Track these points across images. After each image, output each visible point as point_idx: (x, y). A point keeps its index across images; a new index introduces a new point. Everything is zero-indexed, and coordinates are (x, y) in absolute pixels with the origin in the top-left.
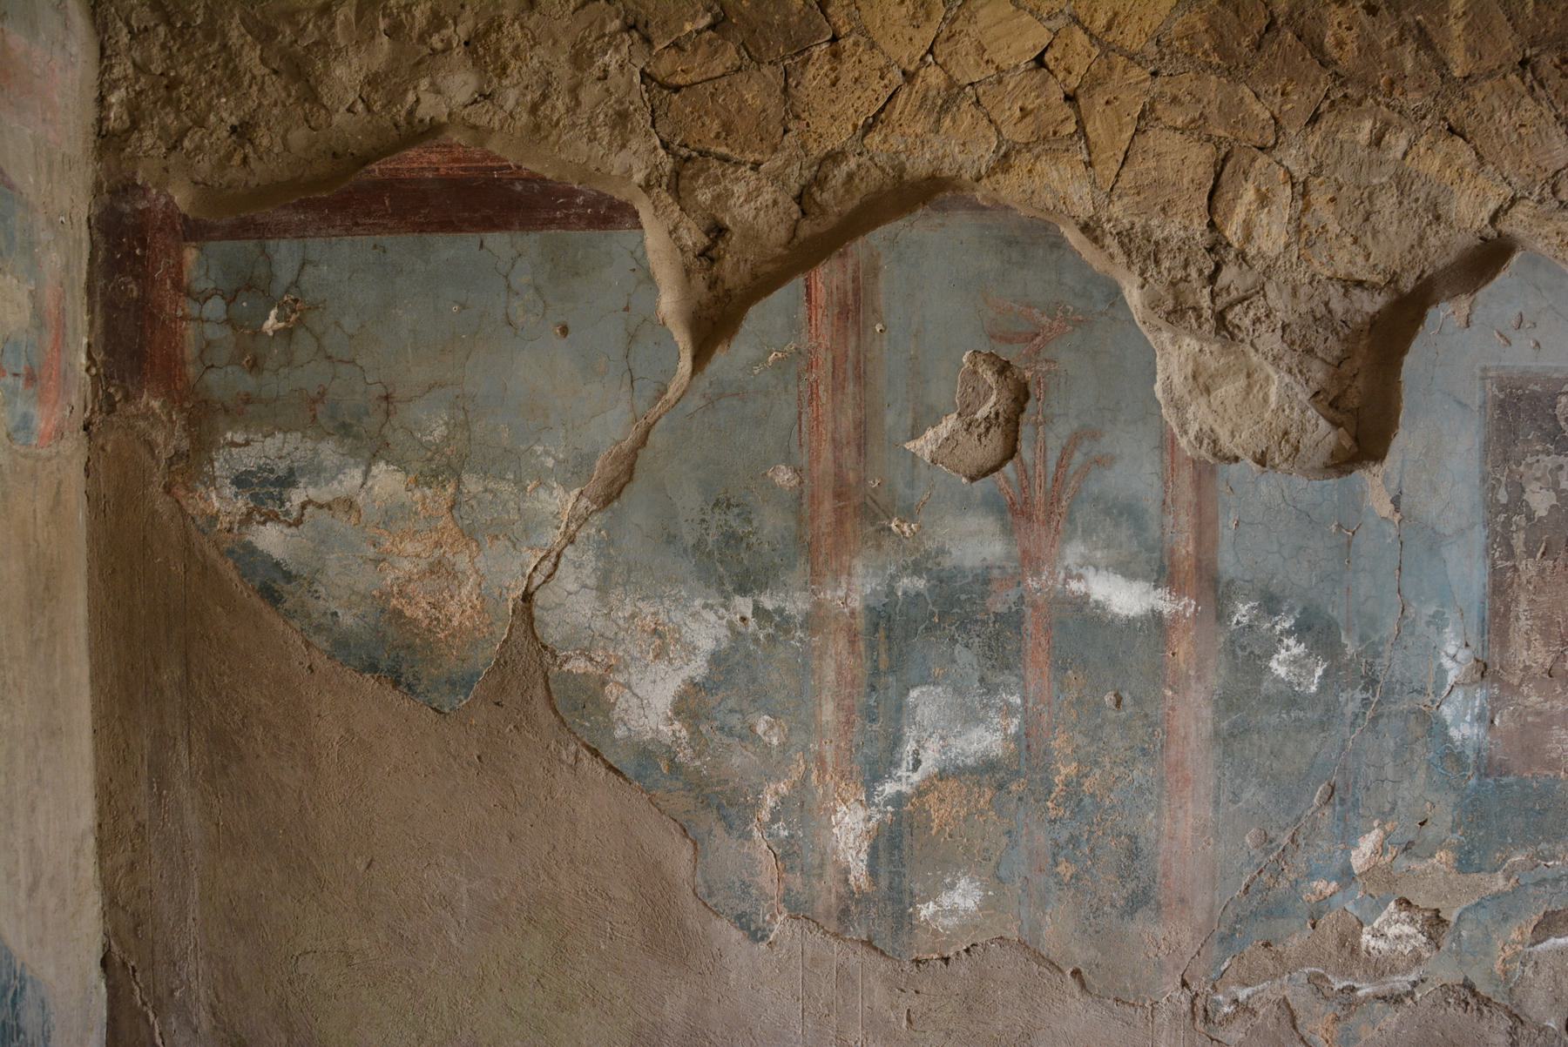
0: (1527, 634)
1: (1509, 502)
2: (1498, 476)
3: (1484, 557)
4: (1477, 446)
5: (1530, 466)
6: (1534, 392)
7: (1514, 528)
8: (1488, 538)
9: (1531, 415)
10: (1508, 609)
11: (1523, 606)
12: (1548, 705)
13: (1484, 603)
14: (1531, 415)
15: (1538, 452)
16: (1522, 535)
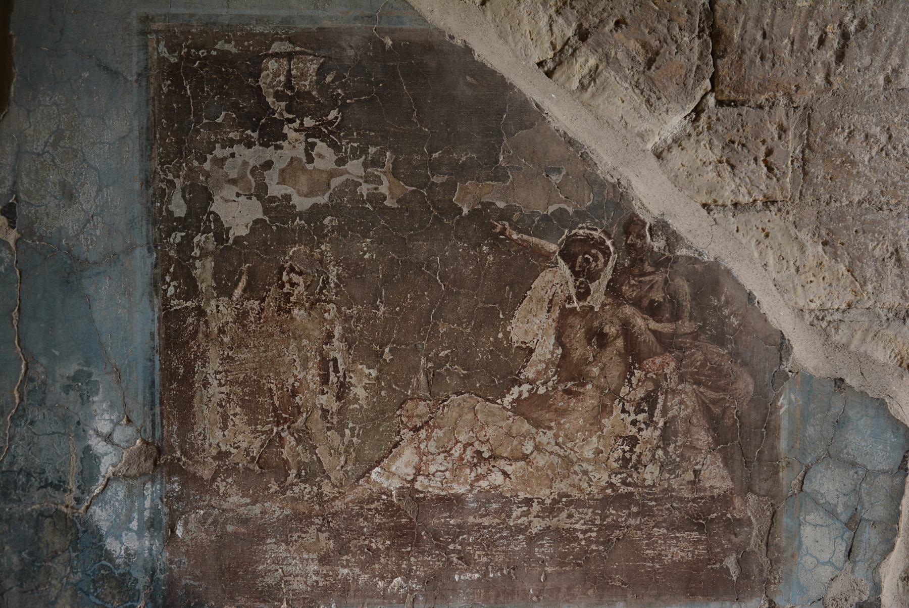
12: (257, 509)
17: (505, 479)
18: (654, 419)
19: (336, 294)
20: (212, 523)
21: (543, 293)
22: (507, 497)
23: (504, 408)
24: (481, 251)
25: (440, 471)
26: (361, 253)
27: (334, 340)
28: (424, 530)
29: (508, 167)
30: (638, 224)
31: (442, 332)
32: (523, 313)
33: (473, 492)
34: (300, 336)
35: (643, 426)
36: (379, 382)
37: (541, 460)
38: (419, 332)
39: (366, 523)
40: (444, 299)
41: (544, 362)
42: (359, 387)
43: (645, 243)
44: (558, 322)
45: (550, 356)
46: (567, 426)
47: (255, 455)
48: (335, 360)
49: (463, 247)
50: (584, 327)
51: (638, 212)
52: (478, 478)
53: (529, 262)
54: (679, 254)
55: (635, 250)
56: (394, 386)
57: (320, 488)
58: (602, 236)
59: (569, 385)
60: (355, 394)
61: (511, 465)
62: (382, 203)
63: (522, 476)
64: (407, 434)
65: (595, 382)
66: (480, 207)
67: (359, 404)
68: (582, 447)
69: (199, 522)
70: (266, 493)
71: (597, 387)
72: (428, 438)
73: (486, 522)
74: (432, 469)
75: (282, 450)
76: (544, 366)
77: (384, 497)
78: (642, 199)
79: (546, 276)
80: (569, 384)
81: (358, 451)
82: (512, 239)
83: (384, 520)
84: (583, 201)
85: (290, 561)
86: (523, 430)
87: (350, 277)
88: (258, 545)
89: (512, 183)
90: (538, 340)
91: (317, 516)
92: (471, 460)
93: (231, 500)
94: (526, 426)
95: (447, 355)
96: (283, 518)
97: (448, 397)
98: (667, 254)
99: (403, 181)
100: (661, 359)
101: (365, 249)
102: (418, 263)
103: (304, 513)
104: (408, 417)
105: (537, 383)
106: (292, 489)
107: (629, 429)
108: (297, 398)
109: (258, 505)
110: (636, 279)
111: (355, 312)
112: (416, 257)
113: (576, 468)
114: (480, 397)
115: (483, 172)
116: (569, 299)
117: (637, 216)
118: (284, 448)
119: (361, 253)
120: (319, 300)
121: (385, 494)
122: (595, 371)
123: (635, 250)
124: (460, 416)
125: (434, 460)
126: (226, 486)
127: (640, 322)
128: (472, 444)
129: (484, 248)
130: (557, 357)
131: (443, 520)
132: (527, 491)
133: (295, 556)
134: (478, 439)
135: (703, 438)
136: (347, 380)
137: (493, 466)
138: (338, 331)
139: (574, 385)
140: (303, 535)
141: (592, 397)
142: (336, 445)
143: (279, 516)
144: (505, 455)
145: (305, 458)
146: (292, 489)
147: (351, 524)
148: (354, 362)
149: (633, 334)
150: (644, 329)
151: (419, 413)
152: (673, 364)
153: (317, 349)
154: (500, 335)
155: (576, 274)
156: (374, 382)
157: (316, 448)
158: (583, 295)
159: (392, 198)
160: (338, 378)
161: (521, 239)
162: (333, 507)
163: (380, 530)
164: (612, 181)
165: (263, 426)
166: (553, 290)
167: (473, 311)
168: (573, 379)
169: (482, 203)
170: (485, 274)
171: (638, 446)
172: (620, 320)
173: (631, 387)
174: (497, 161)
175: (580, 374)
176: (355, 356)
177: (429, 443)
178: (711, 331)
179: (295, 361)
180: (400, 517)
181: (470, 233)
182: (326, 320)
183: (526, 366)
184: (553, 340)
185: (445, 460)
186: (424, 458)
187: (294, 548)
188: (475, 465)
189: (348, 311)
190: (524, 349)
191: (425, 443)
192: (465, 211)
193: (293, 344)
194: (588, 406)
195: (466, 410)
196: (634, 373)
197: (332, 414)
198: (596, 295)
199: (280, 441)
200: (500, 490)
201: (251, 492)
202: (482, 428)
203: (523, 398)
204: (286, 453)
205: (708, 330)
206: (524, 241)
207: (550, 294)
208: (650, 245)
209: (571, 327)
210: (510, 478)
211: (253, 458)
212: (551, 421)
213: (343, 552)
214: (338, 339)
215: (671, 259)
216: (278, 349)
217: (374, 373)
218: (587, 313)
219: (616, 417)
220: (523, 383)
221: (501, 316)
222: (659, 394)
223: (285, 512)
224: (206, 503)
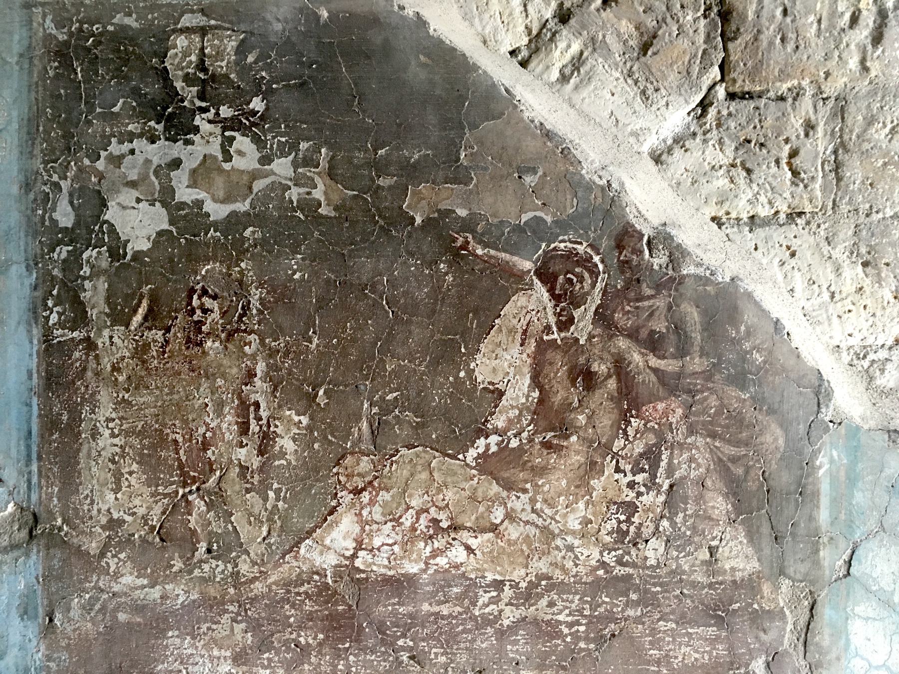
0: (113, 461)
1: (77, 224)
2: (55, 178)
3: (30, 325)
4: (15, 126)
5: (117, 161)
6: (124, 28)
7: (86, 270)
8: (35, 288)
9: (119, 69)
10: (76, 418)
11: (106, 410)
12: (155, 593)
13: (29, 405)
14: (119, 69)
15: (131, 137)
16: (103, 285)
17: (468, 556)
18: (657, 481)
19: (259, 323)
20: (100, 610)
21: (515, 321)
22: (471, 579)
23: (467, 465)
25: (387, 545)
26: (290, 272)
27: (256, 379)
28: (366, 620)
29: (471, 167)
31: (389, 369)
32: (490, 346)
33: (429, 572)
34: (213, 375)
35: (643, 489)
36: (312, 432)
37: (513, 532)
38: (362, 370)
39: (293, 611)
40: (392, 329)
41: (517, 407)
42: (286, 438)
43: (643, 259)
44: (534, 358)
45: (524, 400)
46: (546, 488)
47: (154, 523)
48: (257, 405)
49: (416, 265)
50: (566, 364)
51: (634, 221)
52: (435, 554)
53: (497, 283)
54: (685, 272)
55: (630, 268)
56: (330, 437)
57: (237, 566)
58: (589, 250)
59: (548, 437)
60: (282, 447)
61: (476, 537)
62: (316, 211)
63: (490, 552)
64: (346, 497)
65: (581, 433)
66: (436, 215)
67: (286, 460)
68: (565, 516)
69: (84, 608)
70: (168, 572)
71: (584, 439)
72: (372, 503)
73: (445, 610)
74: (377, 542)
75: (189, 517)
76: (517, 412)
77: (316, 577)
78: (638, 205)
79: (519, 300)
80: (550, 435)
81: (285, 519)
82: (477, 256)
83: (316, 607)
84: (565, 207)
85: (197, 659)
86: (491, 493)
87: (276, 302)
88: (157, 638)
89: (476, 186)
90: (509, 381)
91: (232, 602)
92: (425, 530)
93: (123, 580)
94: (495, 488)
95: (396, 398)
96: (189, 604)
97: (398, 451)
98: (670, 272)
99: (341, 184)
100: (664, 405)
101: (295, 267)
102: (360, 285)
103: (215, 598)
104: (347, 476)
105: (509, 434)
106: (200, 567)
107: (625, 494)
108: (209, 453)
109: (158, 587)
110: (632, 304)
111: (282, 345)
112: (358, 278)
113: (559, 542)
114: (437, 451)
115: (441, 173)
116: (548, 329)
118: (191, 515)
119: (290, 272)
120: (237, 330)
121: (317, 573)
122: (582, 419)
123: (630, 268)
124: (412, 475)
125: (379, 530)
126: (117, 564)
127: (636, 358)
128: (427, 511)
129: (442, 266)
130: (533, 401)
131: (390, 608)
132: (495, 571)
133: (203, 653)
134: (434, 505)
135: (719, 505)
136: (272, 429)
137: (454, 539)
138: (260, 368)
139: (555, 436)
140: (214, 627)
141: (577, 453)
142: (256, 511)
143: (183, 602)
144: (468, 525)
145: (217, 527)
146: (200, 567)
147: (275, 612)
148: (280, 407)
149: (628, 373)
150: (642, 367)
151: (360, 470)
152: (680, 411)
153: (234, 390)
155: (556, 298)
156: (304, 432)
157: (232, 514)
158: (565, 324)
159: (328, 205)
160: (261, 426)
161: (487, 255)
162: (252, 591)
163: (311, 620)
164: (601, 183)
165: (166, 487)
166: (528, 318)
167: (428, 344)
168: (552, 429)
169: (439, 211)
170: (443, 298)
171: (637, 515)
172: (612, 355)
173: (627, 439)
174: (458, 159)
175: (563, 422)
176: (282, 399)
177: (374, 509)
178: (729, 370)
179: (207, 405)
180: (336, 603)
181: (425, 248)
182: (246, 355)
183: (495, 413)
184: (527, 381)
185: (394, 530)
186: (367, 527)
187: (202, 642)
188: (431, 537)
189: (273, 344)
190: (493, 392)
191: (369, 509)
192: (418, 220)
193: (205, 385)
194: (573, 464)
195: (419, 468)
196: (630, 422)
197: (252, 472)
198: (581, 324)
199: (186, 507)
200: (463, 569)
201: (149, 571)
202: (439, 490)
203: (490, 452)
204: (193, 521)
205: (724, 368)
206: (491, 257)
208: (649, 261)
209: (551, 364)
210: (475, 554)
211: (153, 528)
212: (526, 482)
213: (263, 648)
214: (260, 378)
215: (675, 279)
216: (185, 391)
217: (305, 420)
218: (570, 348)
219: (608, 477)
220: (491, 434)
221: (463, 350)
222: (663, 448)
223: (192, 598)
224: (92, 584)
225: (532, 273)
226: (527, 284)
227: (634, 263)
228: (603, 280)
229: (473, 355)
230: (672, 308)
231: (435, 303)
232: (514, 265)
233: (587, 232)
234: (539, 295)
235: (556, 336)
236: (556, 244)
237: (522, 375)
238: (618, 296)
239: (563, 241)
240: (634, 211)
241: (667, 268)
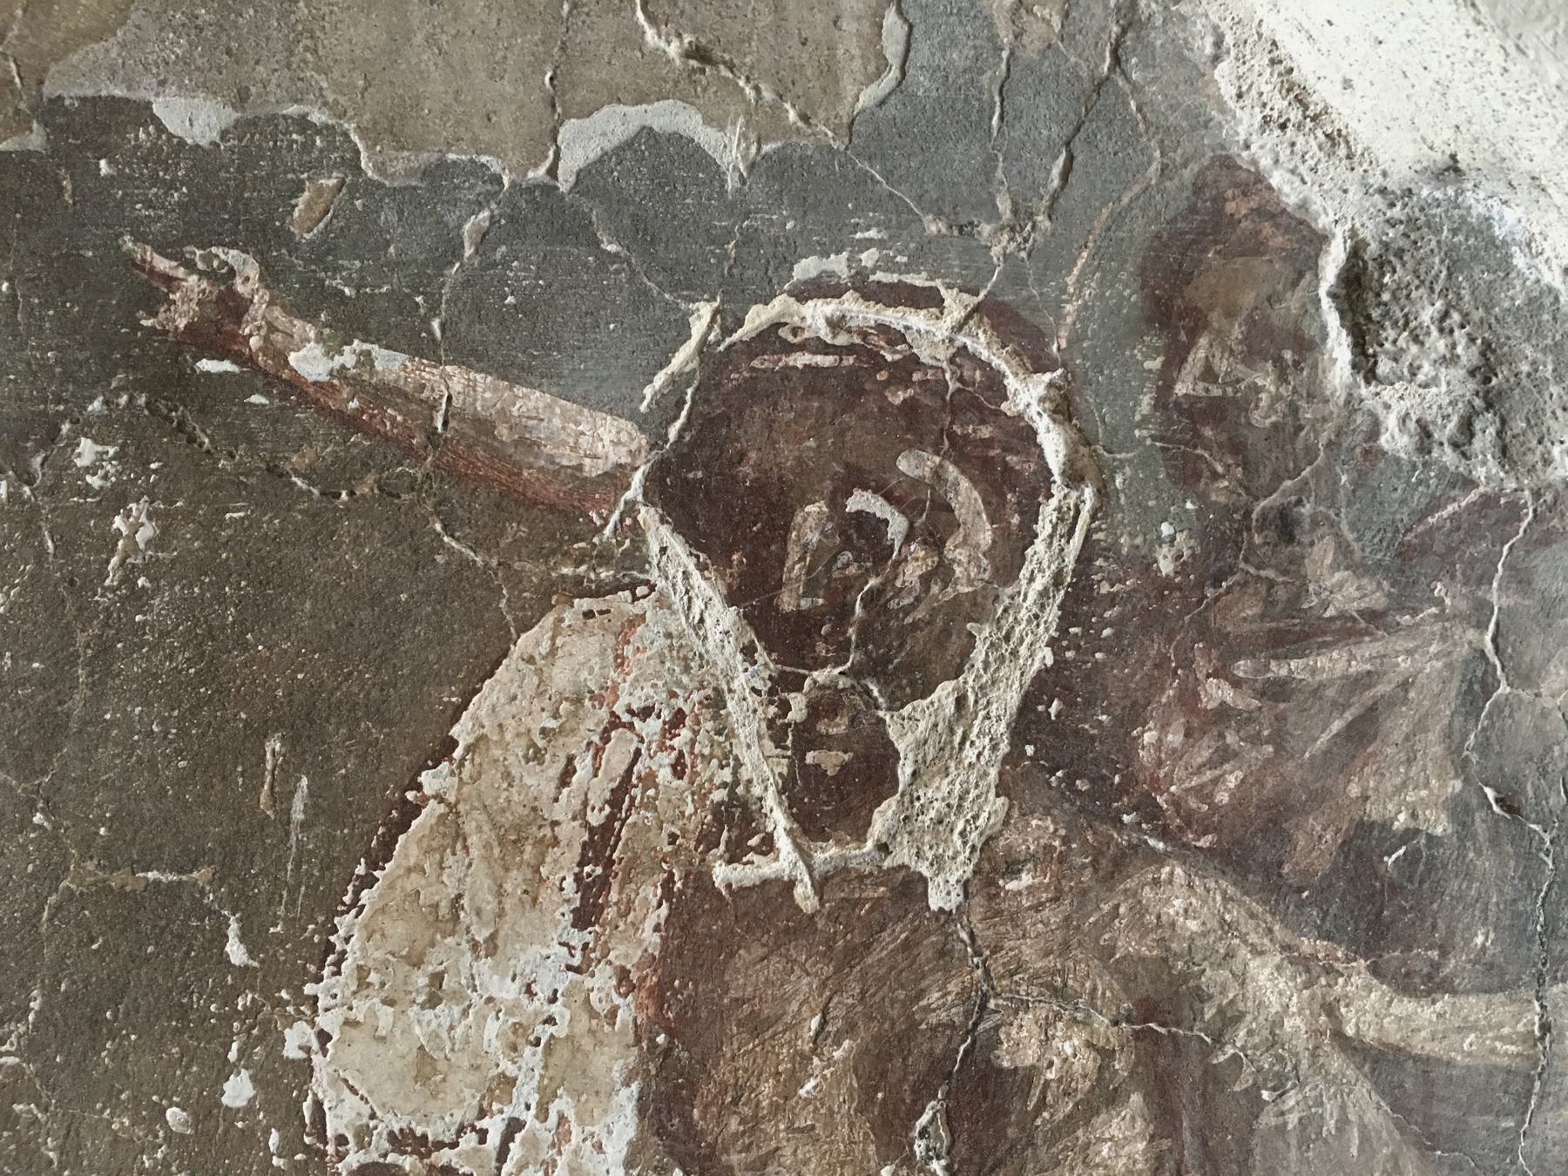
21: (540, 780)
24: (64, 477)
30: (1257, 248)
32: (398, 931)
43: (1314, 393)
44: (659, 995)
50: (850, 1029)
53: (422, 553)
55: (1236, 447)
58: (981, 343)
66: (35, 139)
78: (1292, 46)
82: (294, 386)
84: (830, 72)
90: (514, 1126)
98: (1486, 470)
110: (1242, 667)
117: (1256, 182)
123: (1236, 447)
129: (87, 450)
150: (1302, 1043)
154: (238, 1091)
161: (357, 384)
166: (617, 756)
167: (32, 919)
169: (51, 112)
170: (104, 650)
172: (1124, 972)
198: (937, 792)
206: (383, 394)
207: (592, 783)
208: (1352, 403)
209: (757, 1026)
215: (1515, 511)
221: (236, 952)
225: (635, 491)
226: (604, 558)
227: (1262, 418)
228: (1068, 522)
229: (296, 982)
230: (1488, 689)
231: (57, 680)
232: (527, 444)
233: (965, 230)
234: (679, 623)
235: (785, 860)
236: (780, 304)
237: (591, 1092)
238: (1153, 621)
239: (822, 288)
240: (1266, 84)
241: (1461, 444)
